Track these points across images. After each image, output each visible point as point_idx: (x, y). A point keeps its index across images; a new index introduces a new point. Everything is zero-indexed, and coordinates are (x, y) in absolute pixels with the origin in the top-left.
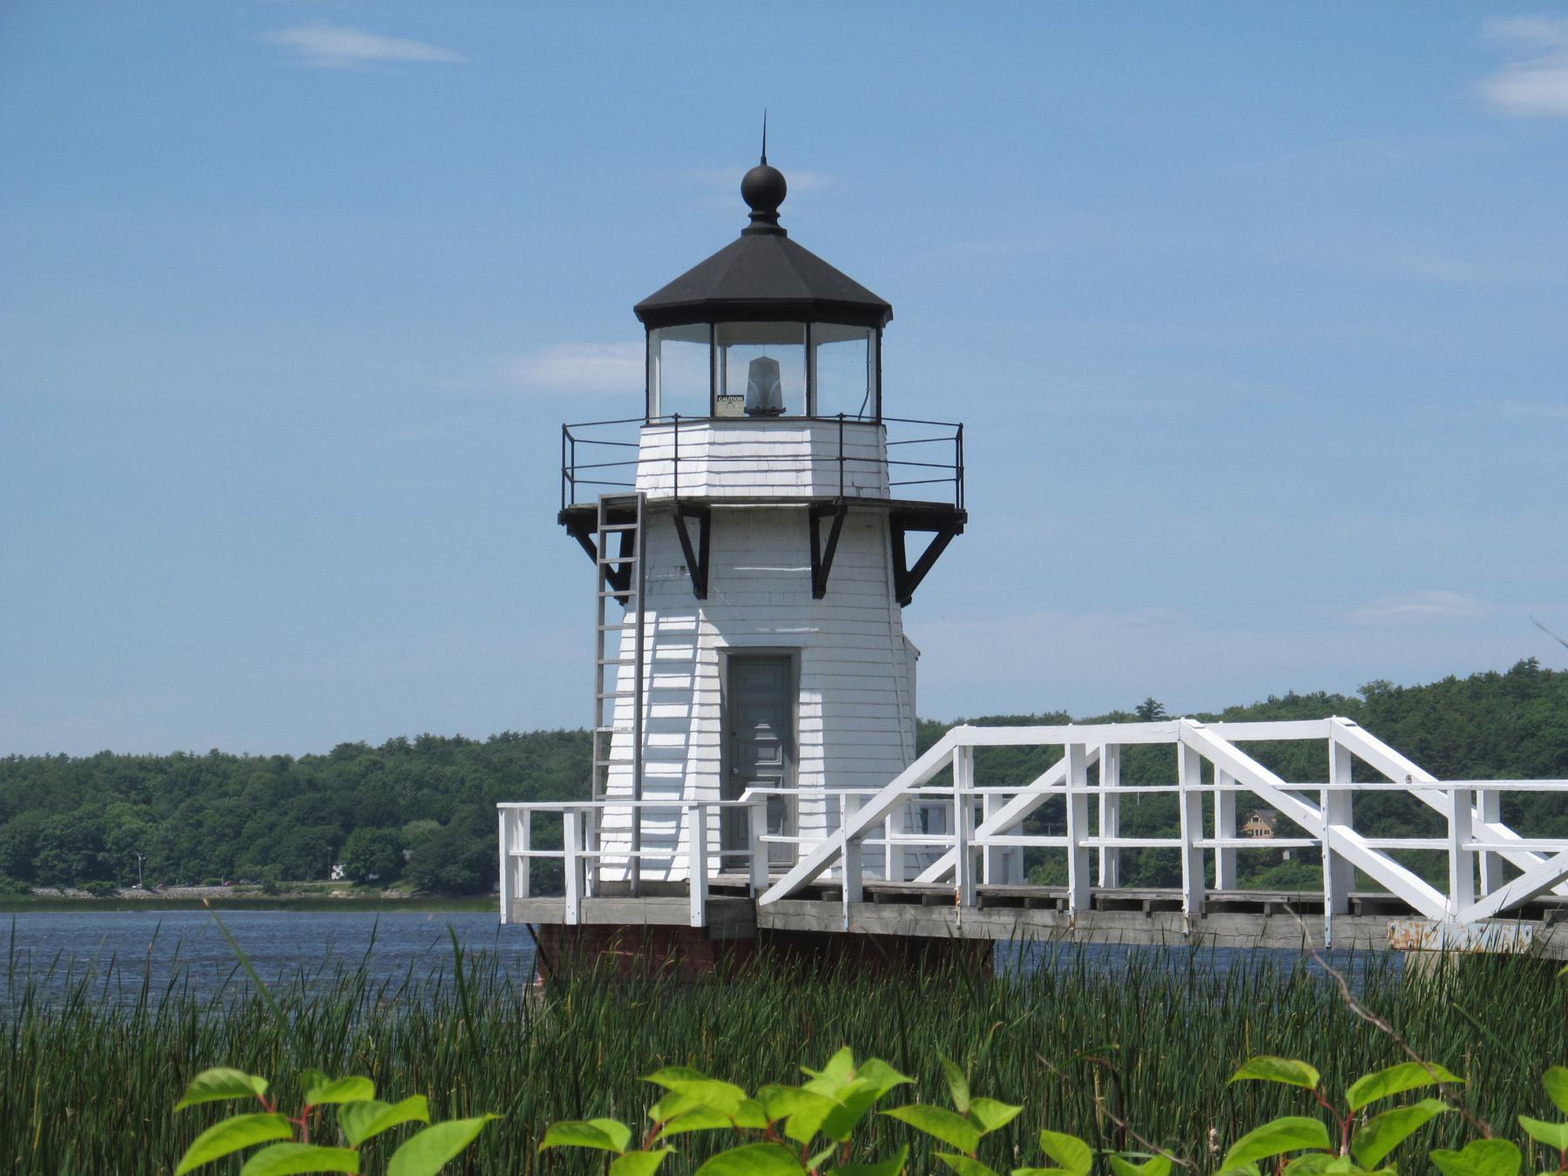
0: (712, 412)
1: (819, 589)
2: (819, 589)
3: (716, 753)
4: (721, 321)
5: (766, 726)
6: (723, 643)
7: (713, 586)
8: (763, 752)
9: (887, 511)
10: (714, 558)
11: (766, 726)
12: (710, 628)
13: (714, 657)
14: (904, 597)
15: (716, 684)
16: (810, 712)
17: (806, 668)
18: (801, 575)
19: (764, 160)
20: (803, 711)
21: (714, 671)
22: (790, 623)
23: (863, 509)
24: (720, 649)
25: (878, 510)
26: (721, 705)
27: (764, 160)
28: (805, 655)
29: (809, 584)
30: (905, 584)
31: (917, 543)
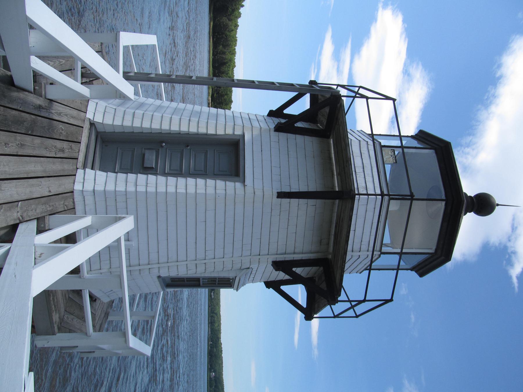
0: (385, 146)
1: (281, 195)
2: (281, 195)
3: (175, 128)
4: (436, 153)
7: (283, 135)
9: (330, 257)
13: (238, 132)
14: (269, 284)
17: (230, 185)
19: (498, 205)
23: (332, 237)
24: (244, 136)
25: (331, 249)
27: (498, 205)
28: (238, 185)
29: (287, 190)
30: (274, 285)
31: (299, 292)
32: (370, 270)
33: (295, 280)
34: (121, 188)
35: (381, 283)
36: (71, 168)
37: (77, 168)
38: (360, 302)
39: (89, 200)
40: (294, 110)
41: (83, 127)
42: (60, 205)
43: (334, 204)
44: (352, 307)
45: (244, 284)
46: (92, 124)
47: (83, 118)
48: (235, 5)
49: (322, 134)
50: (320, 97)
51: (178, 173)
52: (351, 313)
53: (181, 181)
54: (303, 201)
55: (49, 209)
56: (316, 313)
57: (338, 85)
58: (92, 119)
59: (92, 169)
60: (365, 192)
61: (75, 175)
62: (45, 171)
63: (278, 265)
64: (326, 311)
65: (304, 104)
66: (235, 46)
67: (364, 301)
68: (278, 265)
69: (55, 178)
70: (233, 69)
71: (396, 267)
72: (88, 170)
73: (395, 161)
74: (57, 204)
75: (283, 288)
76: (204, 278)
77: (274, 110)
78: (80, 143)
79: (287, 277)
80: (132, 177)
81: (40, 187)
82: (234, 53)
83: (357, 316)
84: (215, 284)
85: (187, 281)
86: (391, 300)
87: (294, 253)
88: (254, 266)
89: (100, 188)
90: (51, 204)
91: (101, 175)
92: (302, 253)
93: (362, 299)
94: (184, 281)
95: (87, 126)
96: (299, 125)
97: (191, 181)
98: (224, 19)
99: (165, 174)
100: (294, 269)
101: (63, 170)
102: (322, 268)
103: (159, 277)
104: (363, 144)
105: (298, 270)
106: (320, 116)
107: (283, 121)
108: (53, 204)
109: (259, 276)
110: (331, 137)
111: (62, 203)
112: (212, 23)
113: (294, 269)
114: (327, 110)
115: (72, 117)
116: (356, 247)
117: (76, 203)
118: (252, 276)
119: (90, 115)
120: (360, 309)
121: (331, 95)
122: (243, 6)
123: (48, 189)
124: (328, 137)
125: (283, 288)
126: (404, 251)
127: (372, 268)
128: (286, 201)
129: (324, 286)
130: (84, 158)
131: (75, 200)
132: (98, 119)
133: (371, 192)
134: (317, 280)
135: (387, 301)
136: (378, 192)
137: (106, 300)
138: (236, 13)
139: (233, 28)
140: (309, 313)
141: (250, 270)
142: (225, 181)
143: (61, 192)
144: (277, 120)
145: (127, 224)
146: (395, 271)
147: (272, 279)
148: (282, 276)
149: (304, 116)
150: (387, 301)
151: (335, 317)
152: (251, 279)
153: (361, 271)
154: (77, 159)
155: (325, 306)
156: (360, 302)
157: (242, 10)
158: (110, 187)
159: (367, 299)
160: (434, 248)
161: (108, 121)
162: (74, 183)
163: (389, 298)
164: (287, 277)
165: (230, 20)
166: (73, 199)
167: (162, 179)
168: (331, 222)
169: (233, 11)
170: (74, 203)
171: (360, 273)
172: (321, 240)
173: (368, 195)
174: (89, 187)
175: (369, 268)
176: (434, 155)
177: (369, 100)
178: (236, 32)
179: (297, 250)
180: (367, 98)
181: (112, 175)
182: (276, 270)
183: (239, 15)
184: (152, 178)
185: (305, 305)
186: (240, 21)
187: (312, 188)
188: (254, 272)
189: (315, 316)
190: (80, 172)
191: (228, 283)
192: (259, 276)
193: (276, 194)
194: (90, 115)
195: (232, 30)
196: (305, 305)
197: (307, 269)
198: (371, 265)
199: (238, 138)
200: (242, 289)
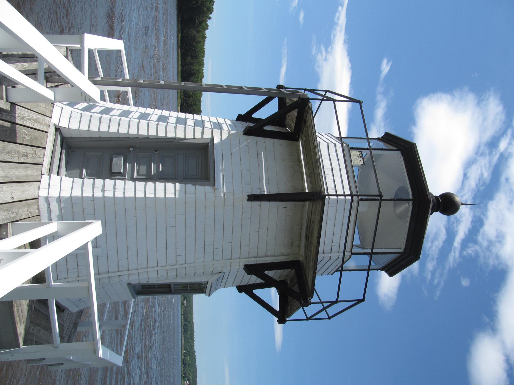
1: (252, 198)
2: (252, 198)
5: (161, 169)
6: (216, 142)
7: (252, 139)
8: (143, 168)
9: (301, 259)
10: (269, 142)
11: (161, 169)
12: (225, 136)
13: (207, 136)
14: (241, 289)
15: (189, 136)
16: (168, 190)
17: (200, 189)
18: (261, 188)
19: (462, 204)
20: (170, 186)
21: (198, 135)
22: (229, 180)
23: (303, 240)
24: (212, 139)
25: (302, 251)
26: (175, 139)
28: (208, 189)
29: (257, 192)
30: (246, 289)
31: (272, 296)
32: (342, 271)
33: (268, 283)
34: (88, 193)
35: (352, 284)
36: (36, 174)
37: (42, 174)
38: (332, 303)
39: (55, 207)
40: (262, 114)
41: (47, 132)
42: (23, 211)
43: (304, 205)
44: (325, 309)
45: (216, 289)
46: (57, 129)
47: (48, 123)
48: (203, 18)
49: (292, 137)
50: (288, 101)
51: (148, 178)
52: (323, 315)
53: (150, 185)
54: (273, 204)
55: (11, 216)
56: (289, 316)
57: (305, 90)
58: (57, 124)
59: (58, 175)
60: (335, 193)
61: (40, 181)
62: (6, 177)
63: (250, 269)
64: (299, 314)
65: (272, 108)
66: (203, 57)
67: (337, 302)
68: (250, 269)
69: (18, 184)
70: (201, 79)
71: (367, 268)
72: (54, 176)
73: (362, 163)
74: (20, 210)
75: (255, 292)
76: (175, 284)
77: (243, 114)
78: (45, 148)
79: (259, 281)
80: (99, 182)
81: (2, 193)
82: (202, 64)
83: (329, 318)
84: (187, 290)
85: (158, 288)
86: (363, 300)
87: (266, 256)
88: (226, 270)
89: (66, 194)
90: (14, 211)
91: (67, 181)
92: (274, 256)
93: (335, 299)
94: (155, 288)
95: (52, 131)
96: (267, 128)
97: (160, 185)
98: (192, 31)
99: (133, 179)
100: (266, 272)
101: (27, 176)
102: (294, 271)
103: (129, 284)
104: (332, 146)
105: (270, 273)
106: (288, 120)
107: (252, 125)
108: (16, 210)
109: (231, 280)
110: (300, 140)
111: (26, 209)
112: (180, 35)
113: (266, 272)
114: (295, 113)
115: (36, 122)
116: (327, 248)
117: (41, 210)
118: (224, 280)
119: (55, 120)
120: (332, 311)
121: (299, 98)
122: (210, 18)
123: (10, 195)
124: (297, 140)
125: (255, 292)
126: (374, 251)
127: (343, 269)
128: (256, 204)
129: (296, 288)
130: (49, 164)
131: (40, 207)
132: (64, 124)
133: (340, 192)
134: (289, 283)
135: (359, 301)
136: (348, 192)
137: (74, 309)
138: (203, 25)
139: (201, 39)
140: (282, 316)
141: (222, 274)
142: (195, 184)
143: (24, 199)
144: (245, 125)
145: (95, 229)
146: (367, 271)
147: (243, 283)
148: (254, 279)
149: (272, 120)
150: (359, 301)
151: (308, 319)
152: (223, 284)
153: (332, 272)
154: (42, 164)
155: (298, 308)
156: (332, 303)
157: (209, 22)
158: (77, 193)
159: (339, 300)
160: (403, 247)
161: (74, 126)
162: (39, 190)
163: (361, 298)
164: (259, 281)
165: (198, 32)
166: (38, 206)
167: (130, 184)
168: (302, 225)
169: (201, 23)
170: (39, 209)
171: (332, 274)
172: (292, 243)
173: (337, 195)
174: (54, 193)
175: (340, 269)
176: (400, 156)
177: (337, 103)
178: (204, 43)
179: (269, 253)
180: (334, 101)
181: (78, 181)
182: (248, 274)
183: (207, 27)
184: (120, 183)
185: (278, 309)
186: (208, 33)
187: (283, 189)
188: (226, 277)
189: (288, 319)
190: (45, 179)
191: (200, 288)
192: (231, 280)
193: (247, 197)
194: (55, 120)
195: (200, 42)
196: (278, 309)
197: (279, 272)
198: (342, 266)
199: (208, 141)
200: (214, 294)
